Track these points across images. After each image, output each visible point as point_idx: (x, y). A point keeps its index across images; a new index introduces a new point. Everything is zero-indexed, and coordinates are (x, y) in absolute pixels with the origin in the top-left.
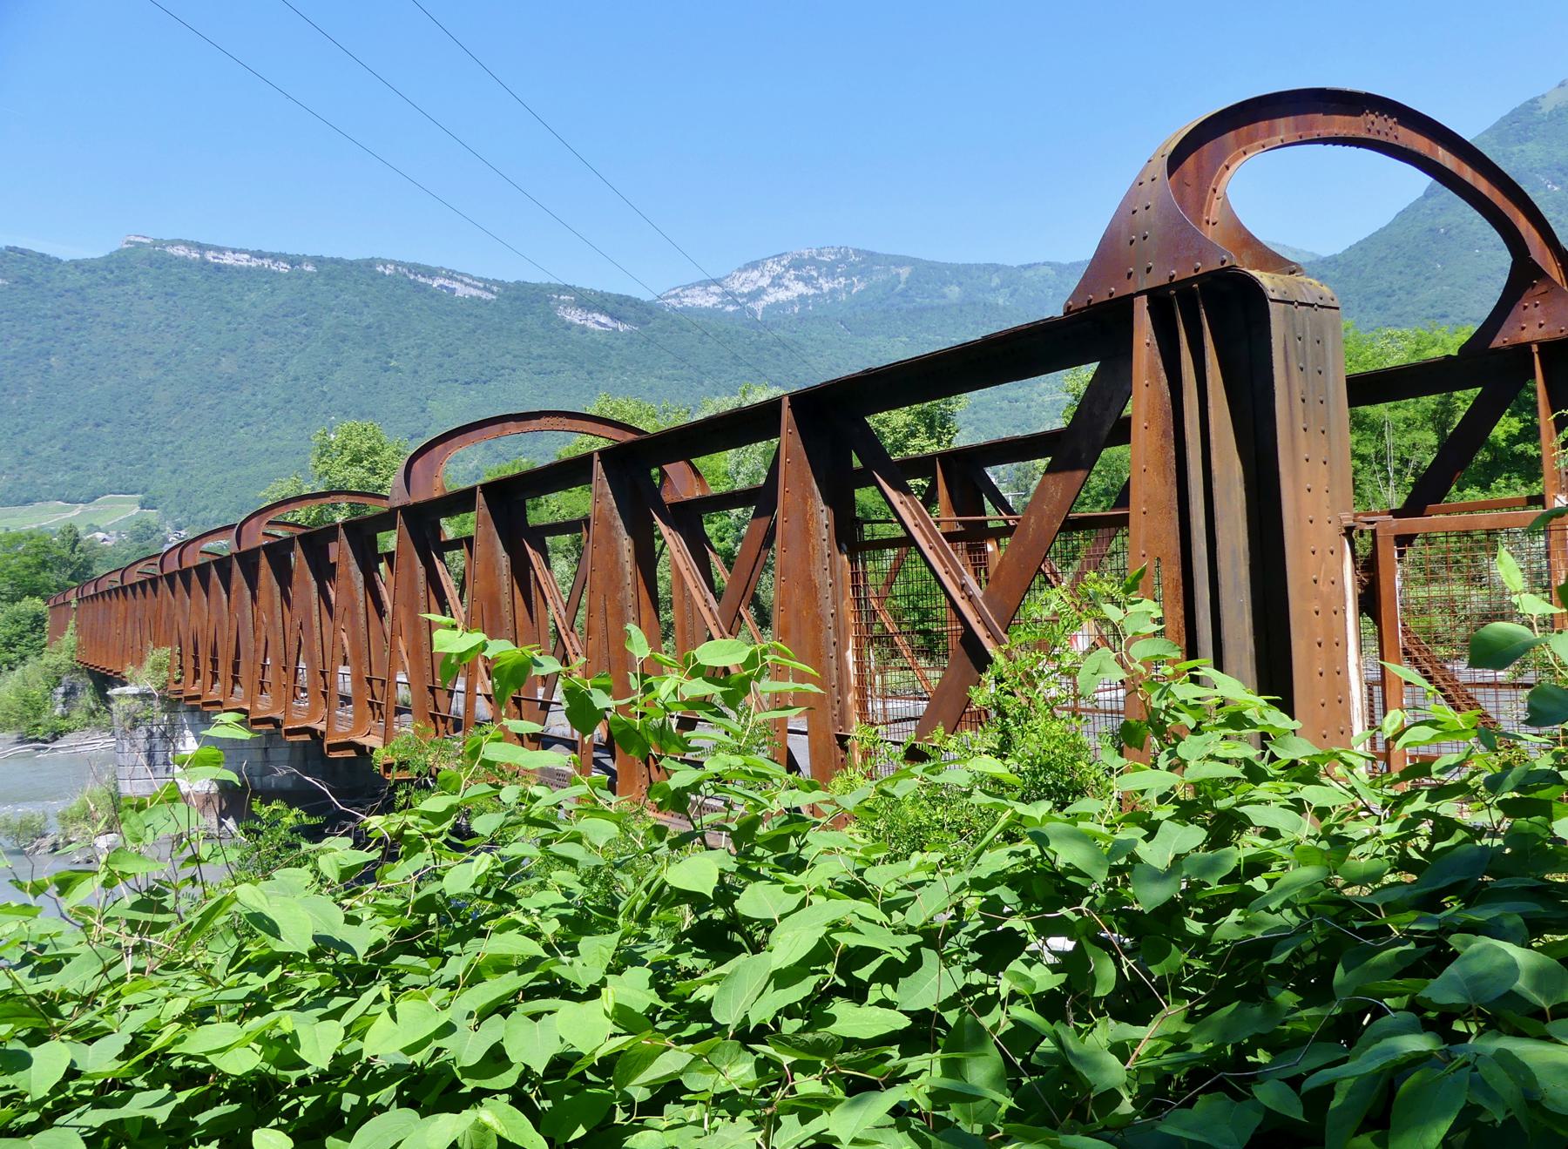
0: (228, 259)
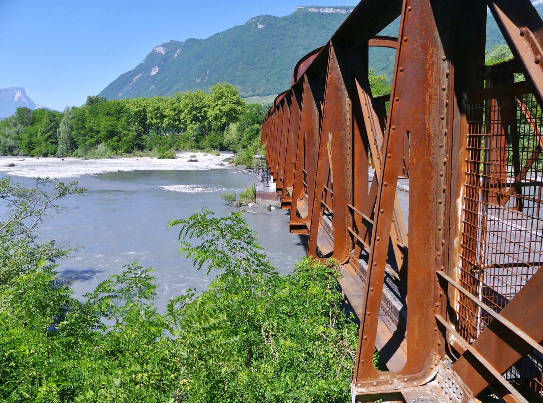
0: (326, 11)
